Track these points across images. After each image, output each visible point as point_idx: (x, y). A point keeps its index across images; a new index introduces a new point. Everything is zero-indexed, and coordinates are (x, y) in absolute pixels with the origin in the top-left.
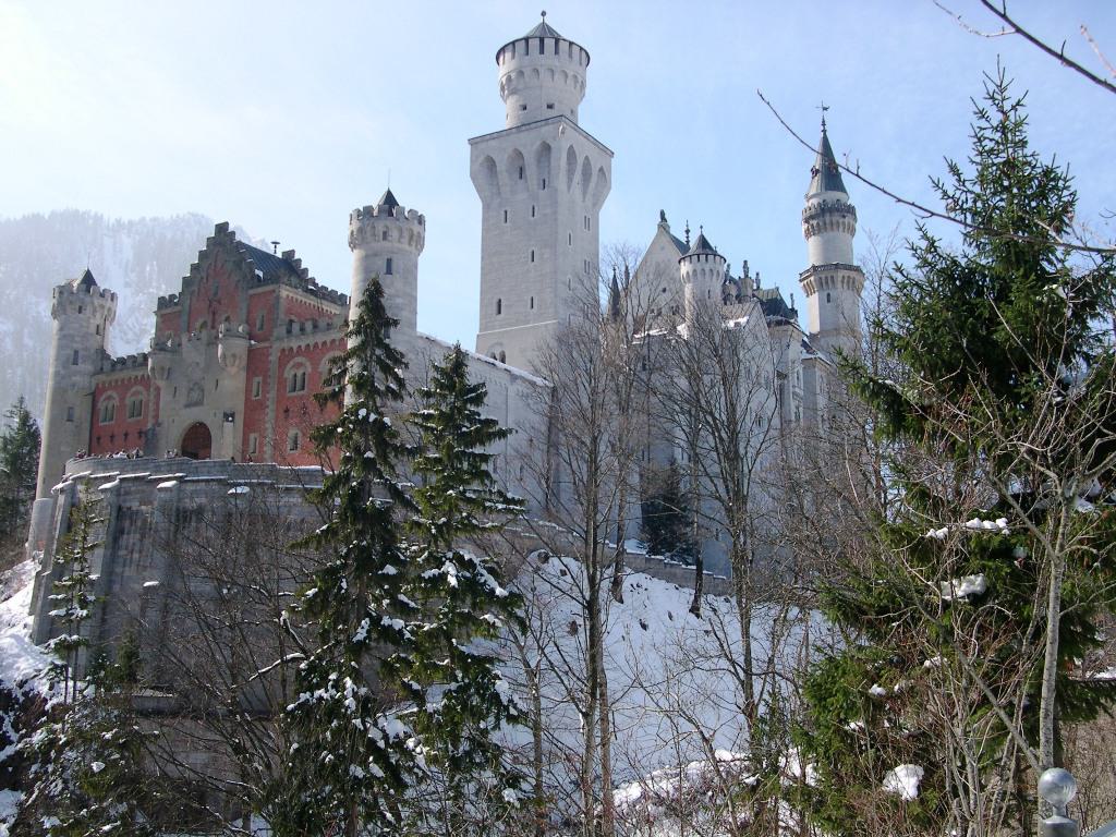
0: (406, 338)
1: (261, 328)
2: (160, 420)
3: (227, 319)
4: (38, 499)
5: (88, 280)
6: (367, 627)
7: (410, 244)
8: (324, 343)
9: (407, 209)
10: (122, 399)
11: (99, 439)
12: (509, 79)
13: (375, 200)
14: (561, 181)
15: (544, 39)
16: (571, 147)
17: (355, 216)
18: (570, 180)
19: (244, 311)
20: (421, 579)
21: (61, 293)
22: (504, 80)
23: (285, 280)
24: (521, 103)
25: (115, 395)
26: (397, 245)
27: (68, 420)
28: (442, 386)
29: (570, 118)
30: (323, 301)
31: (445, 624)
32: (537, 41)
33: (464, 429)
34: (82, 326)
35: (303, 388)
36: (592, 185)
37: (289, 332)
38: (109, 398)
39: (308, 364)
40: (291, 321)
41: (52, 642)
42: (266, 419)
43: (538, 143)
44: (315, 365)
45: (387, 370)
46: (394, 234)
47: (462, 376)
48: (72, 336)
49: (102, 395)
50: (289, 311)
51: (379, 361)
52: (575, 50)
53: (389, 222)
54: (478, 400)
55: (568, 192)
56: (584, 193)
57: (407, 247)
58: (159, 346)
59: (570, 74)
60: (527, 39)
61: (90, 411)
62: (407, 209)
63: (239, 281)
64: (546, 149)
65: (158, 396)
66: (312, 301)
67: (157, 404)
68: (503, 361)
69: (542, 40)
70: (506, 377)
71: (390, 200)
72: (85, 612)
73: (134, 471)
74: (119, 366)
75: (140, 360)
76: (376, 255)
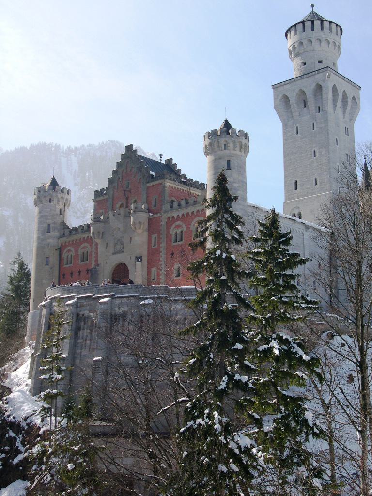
0: (241, 207)
1: (155, 206)
2: (99, 262)
3: (135, 201)
4: (31, 311)
5: (54, 183)
6: (226, 381)
7: (240, 151)
8: (193, 213)
9: (238, 130)
10: (76, 251)
11: (64, 275)
12: (294, 47)
13: (218, 126)
14: (329, 107)
15: (314, 21)
16: (334, 86)
17: (207, 136)
18: (335, 106)
19: (145, 196)
20: (257, 351)
21: (39, 191)
22: (291, 48)
23: (168, 176)
24: (302, 61)
25: (72, 249)
26: (233, 152)
27: (46, 265)
28: (265, 235)
29: (332, 68)
30: (192, 188)
31: (273, 378)
32: (310, 23)
33: (279, 260)
34: (51, 210)
35: (182, 240)
36: (349, 108)
37: (172, 207)
39: (184, 226)
40: (173, 201)
41: (42, 394)
42: (161, 259)
43: (314, 85)
44: (188, 226)
45: (232, 227)
46: (231, 145)
47: (277, 228)
48: (48, 216)
49: (64, 250)
50: (171, 195)
51: (227, 222)
52: (333, 26)
53: (227, 138)
54: (287, 242)
55: (334, 114)
56: (344, 113)
57: (238, 152)
58: (96, 219)
59: (331, 41)
60: (303, 22)
61: (58, 259)
62: (238, 130)
63: (141, 178)
64: (319, 88)
65: (97, 248)
66: (184, 188)
67: (97, 253)
68: (300, 218)
69: (312, 22)
70: (303, 227)
71: (227, 125)
72: (60, 376)
73: (86, 293)
74: (74, 232)
75: (86, 228)
76: (220, 159)
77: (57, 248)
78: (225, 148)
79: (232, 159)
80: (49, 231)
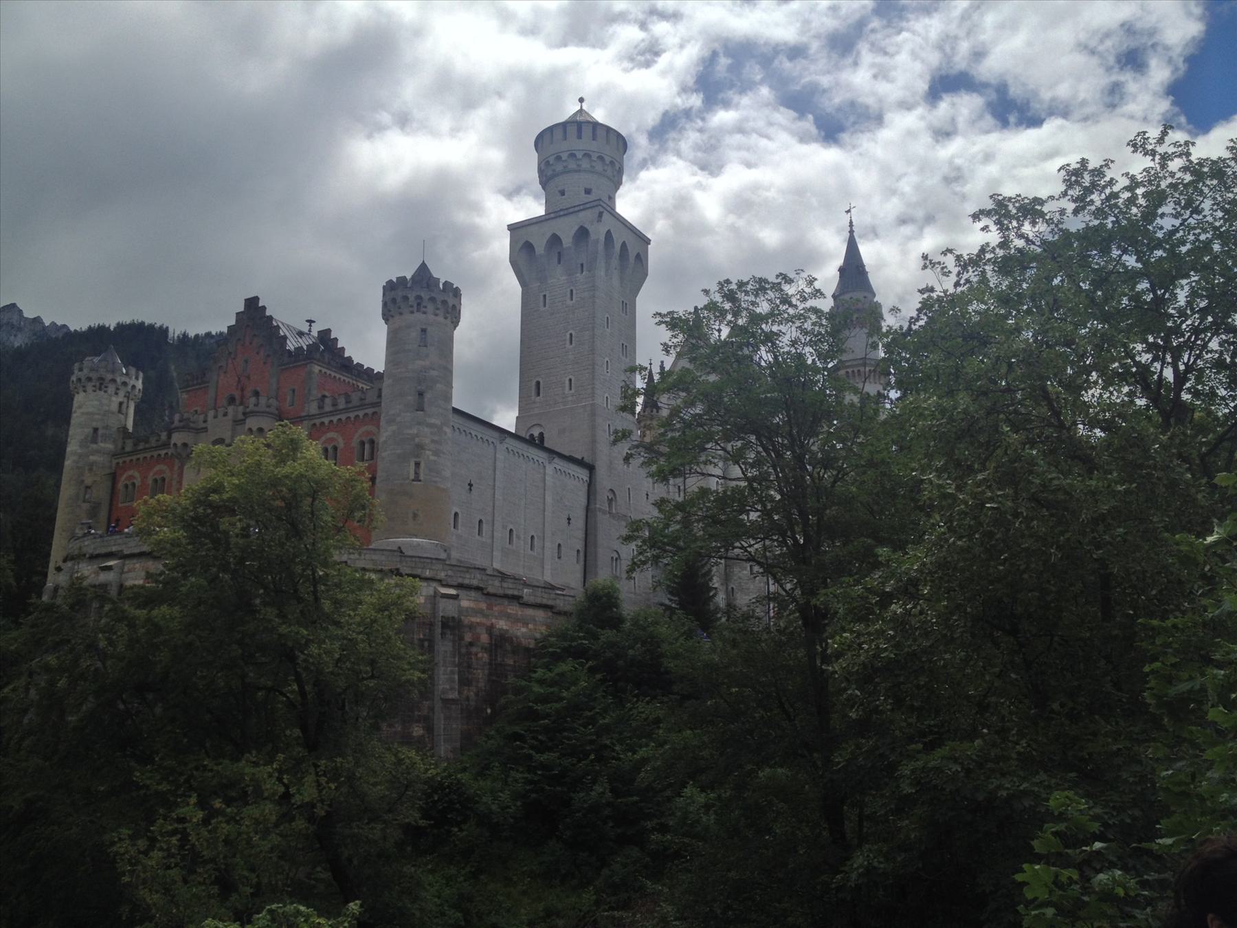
3: (257, 394)
9: (442, 281)
11: (118, 521)
25: (137, 474)
29: (605, 207)
37: (320, 407)
38: (131, 477)
40: (324, 396)
43: (576, 228)
53: (425, 295)
57: (441, 319)
59: (608, 159)
62: (442, 281)
64: (583, 233)
65: (181, 475)
71: (423, 268)
77: (108, 471)
78: (418, 310)
79: (429, 329)
80: (94, 441)
